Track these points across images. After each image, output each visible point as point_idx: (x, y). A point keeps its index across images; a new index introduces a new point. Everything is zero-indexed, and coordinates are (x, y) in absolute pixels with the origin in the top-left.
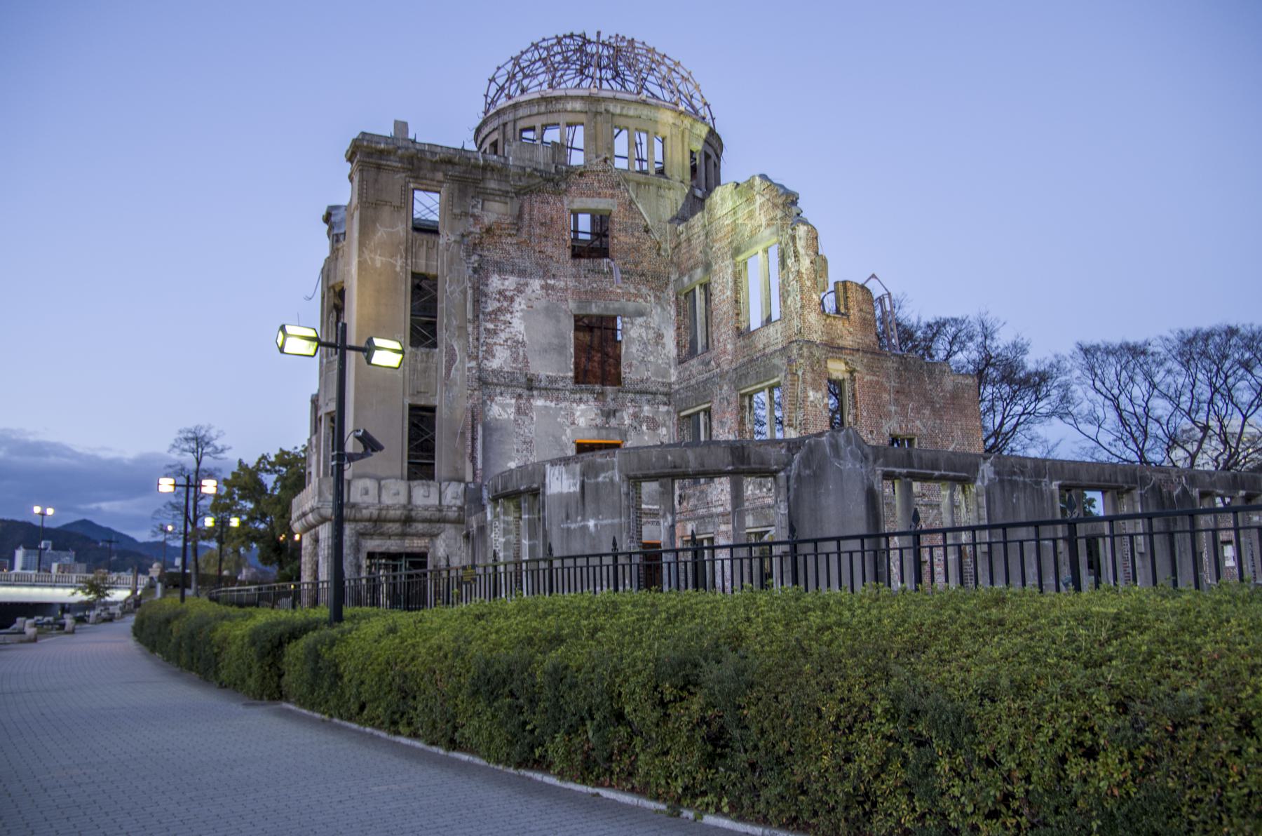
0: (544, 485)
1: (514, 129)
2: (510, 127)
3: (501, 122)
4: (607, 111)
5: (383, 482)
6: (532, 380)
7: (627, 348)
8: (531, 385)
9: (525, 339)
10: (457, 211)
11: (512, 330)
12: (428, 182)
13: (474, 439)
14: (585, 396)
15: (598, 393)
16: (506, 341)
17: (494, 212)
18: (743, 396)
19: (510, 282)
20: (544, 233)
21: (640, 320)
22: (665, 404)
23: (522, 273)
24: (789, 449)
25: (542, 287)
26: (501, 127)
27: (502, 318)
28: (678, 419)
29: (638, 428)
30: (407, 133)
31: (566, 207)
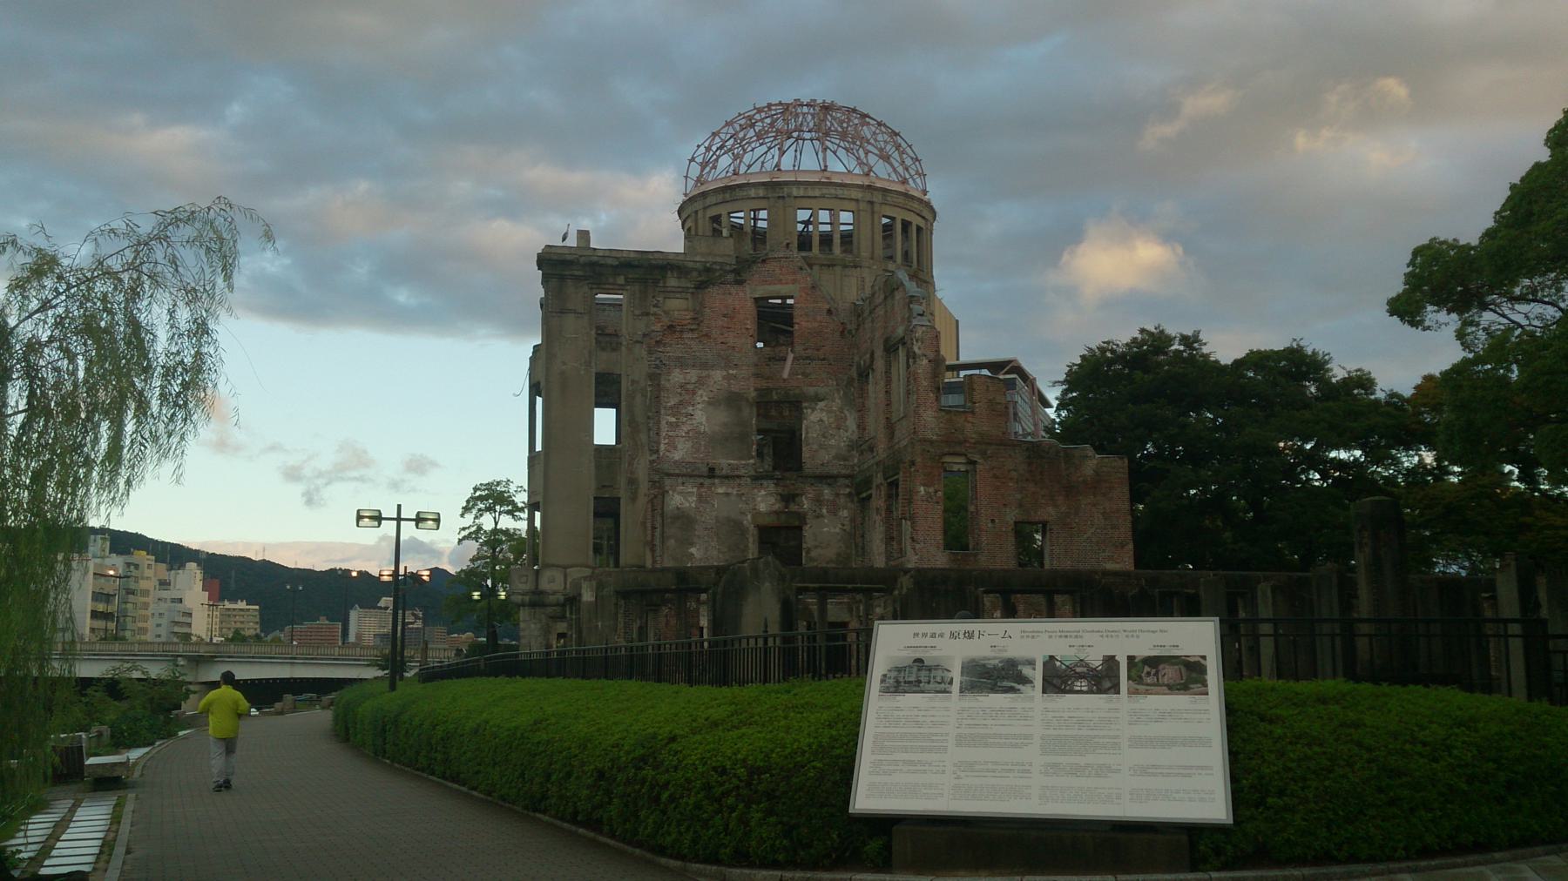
0: (580, 595)
1: (704, 217)
2: (700, 214)
3: (694, 209)
4: (789, 196)
5: (568, 570)
6: (714, 469)
7: (807, 433)
8: (712, 472)
9: (706, 430)
10: (637, 312)
11: (694, 422)
12: (611, 287)
13: (654, 528)
14: (765, 483)
15: (777, 479)
16: (686, 433)
17: (677, 306)
18: (890, 484)
19: (693, 375)
20: (725, 325)
21: (821, 404)
22: (848, 486)
23: (705, 366)
24: (717, 573)
25: (724, 378)
26: (693, 214)
27: (684, 411)
28: (858, 502)
29: (818, 511)
30: (588, 241)
31: (748, 296)
